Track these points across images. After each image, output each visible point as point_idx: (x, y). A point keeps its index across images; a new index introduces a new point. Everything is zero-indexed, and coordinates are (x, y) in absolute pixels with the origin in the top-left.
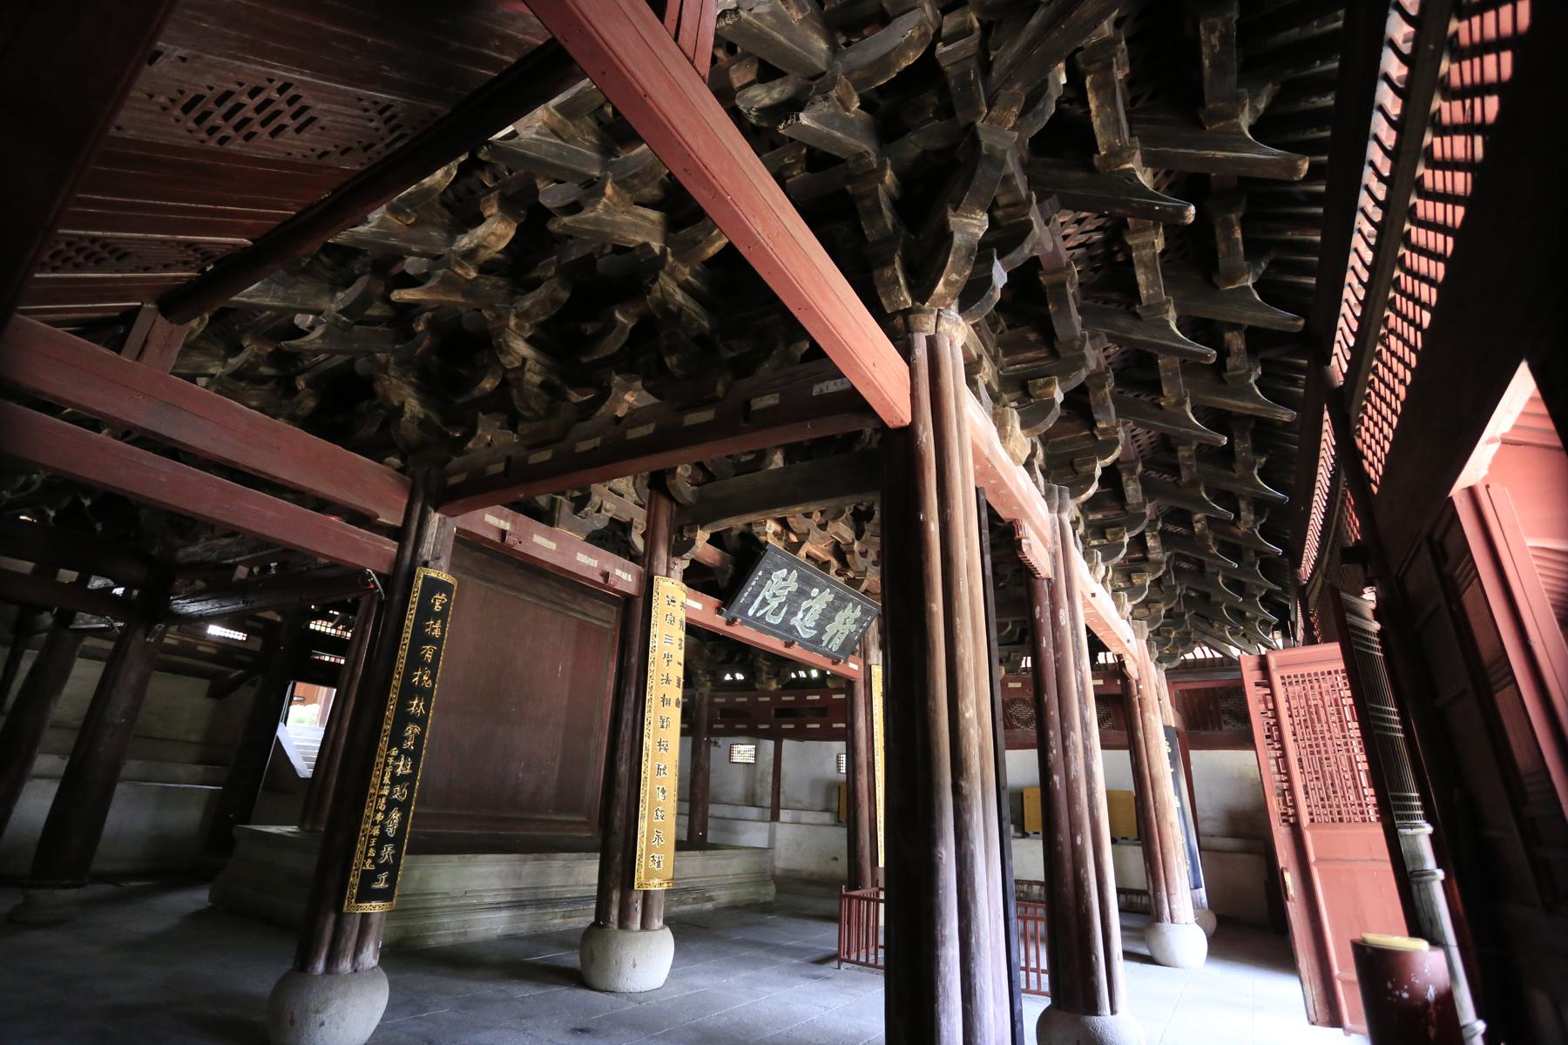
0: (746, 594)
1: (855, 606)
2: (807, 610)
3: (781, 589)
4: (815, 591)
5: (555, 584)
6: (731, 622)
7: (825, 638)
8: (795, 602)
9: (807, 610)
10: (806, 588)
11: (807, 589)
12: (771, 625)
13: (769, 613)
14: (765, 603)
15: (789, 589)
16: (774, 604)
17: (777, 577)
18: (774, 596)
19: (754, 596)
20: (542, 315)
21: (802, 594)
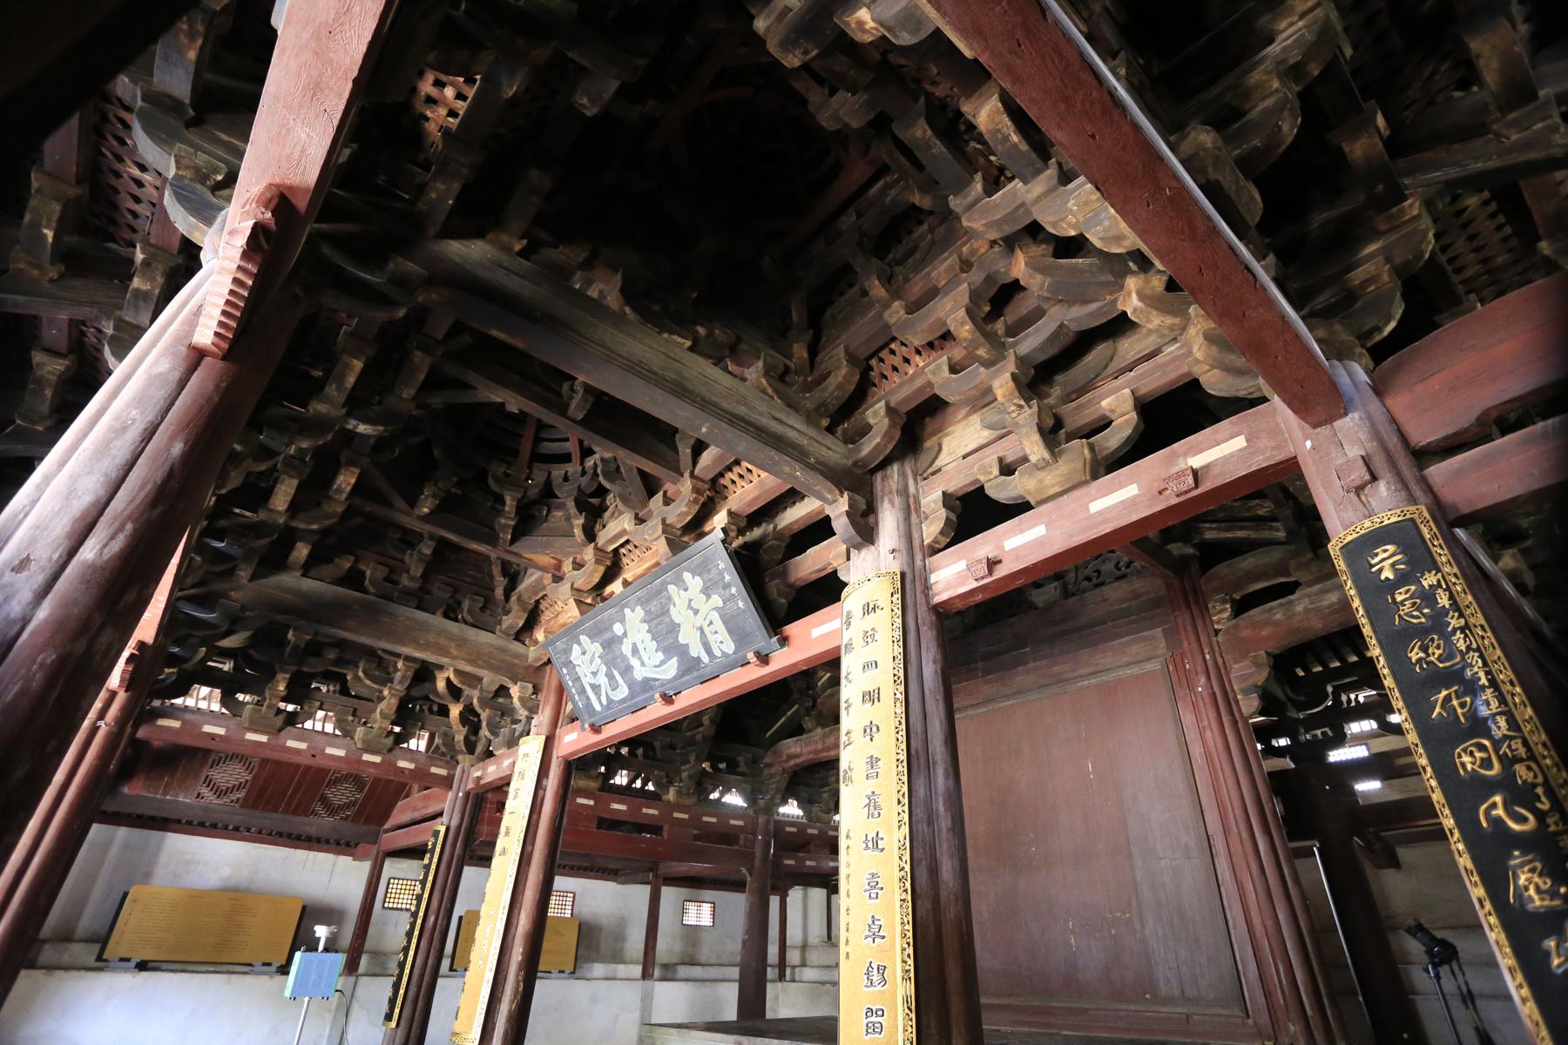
0: (576, 697)
1: (679, 582)
2: (635, 651)
3: (591, 663)
4: (618, 629)
5: (1038, 663)
6: (596, 729)
7: (696, 650)
8: (616, 658)
9: (635, 651)
10: (607, 635)
11: (607, 635)
12: (624, 700)
13: (610, 692)
14: (596, 688)
15: (596, 655)
16: (602, 680)
17: (576, 658)
18: (594, 674)
19: (583, 691)
20: (889, 443)
21: (611, 644)
